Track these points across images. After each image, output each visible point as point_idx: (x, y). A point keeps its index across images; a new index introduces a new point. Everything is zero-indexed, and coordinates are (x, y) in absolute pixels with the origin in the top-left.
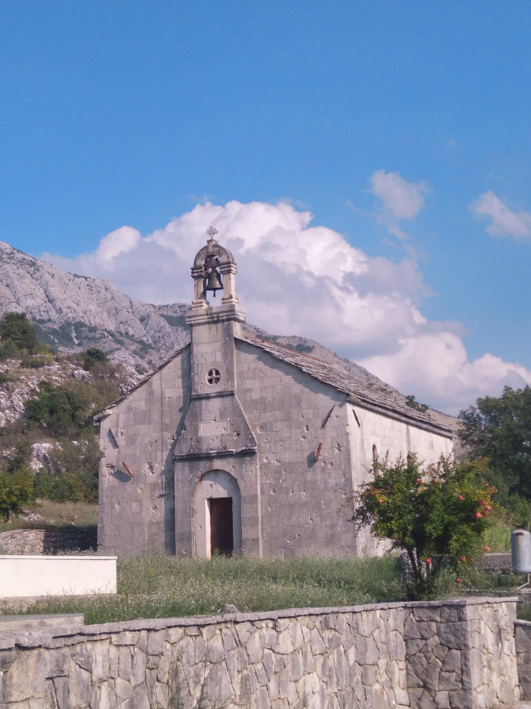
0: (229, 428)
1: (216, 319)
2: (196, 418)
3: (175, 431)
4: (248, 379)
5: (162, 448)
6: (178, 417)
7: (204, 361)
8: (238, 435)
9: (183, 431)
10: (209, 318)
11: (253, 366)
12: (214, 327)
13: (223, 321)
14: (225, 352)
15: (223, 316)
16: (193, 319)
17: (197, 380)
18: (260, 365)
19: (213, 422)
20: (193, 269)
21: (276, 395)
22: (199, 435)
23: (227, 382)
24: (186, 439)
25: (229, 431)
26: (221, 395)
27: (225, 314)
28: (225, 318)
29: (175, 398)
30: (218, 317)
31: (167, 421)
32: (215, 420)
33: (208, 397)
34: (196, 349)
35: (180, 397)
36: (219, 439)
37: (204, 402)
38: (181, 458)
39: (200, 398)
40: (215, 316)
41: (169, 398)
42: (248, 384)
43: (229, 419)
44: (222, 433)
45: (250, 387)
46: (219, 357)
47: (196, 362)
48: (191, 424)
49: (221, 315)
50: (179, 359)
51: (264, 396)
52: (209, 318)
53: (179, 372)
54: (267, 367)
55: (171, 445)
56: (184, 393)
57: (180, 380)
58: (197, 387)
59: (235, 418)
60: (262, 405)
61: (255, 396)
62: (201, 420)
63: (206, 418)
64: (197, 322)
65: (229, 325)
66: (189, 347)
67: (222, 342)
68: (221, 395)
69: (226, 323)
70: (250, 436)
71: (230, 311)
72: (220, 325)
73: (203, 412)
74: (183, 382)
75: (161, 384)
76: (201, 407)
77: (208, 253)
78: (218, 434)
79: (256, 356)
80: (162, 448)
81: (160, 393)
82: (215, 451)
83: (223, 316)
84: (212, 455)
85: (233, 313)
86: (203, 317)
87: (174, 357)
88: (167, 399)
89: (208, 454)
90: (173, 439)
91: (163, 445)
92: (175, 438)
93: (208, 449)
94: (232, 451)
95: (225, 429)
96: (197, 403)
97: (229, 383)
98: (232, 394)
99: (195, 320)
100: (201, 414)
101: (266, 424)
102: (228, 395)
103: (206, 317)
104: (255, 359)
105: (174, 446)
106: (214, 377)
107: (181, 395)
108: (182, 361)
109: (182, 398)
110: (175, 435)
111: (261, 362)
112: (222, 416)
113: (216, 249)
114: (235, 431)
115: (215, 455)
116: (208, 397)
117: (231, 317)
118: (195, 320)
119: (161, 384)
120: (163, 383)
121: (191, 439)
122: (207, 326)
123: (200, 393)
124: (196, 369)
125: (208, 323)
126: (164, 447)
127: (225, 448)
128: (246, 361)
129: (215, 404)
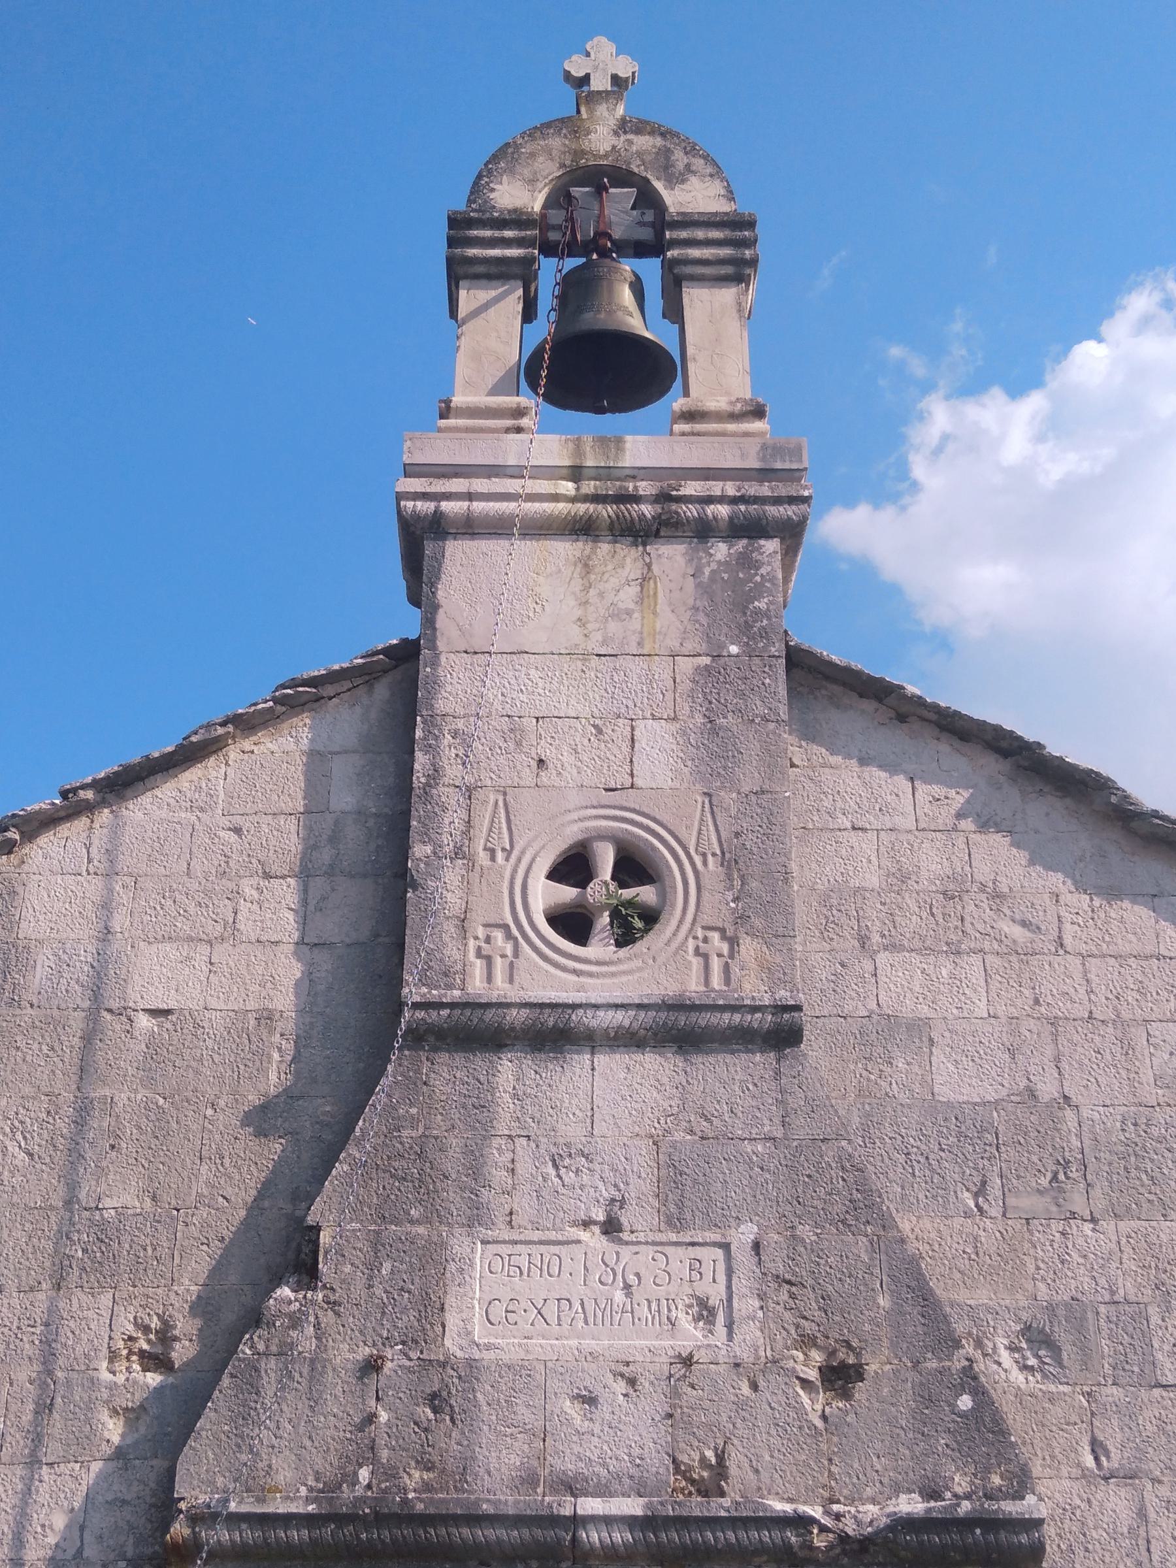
0: (747, 1304)
1: (647, 510)
2: (435, 1194)
3: (189, 1287)
4: (893, 947)
5: (37, 1439)
6: (227, 1179)
7: (528, 777)
8: (840, 1377)
9: (285, 1292)
10: (596, 499)
11: (932, 862)
12: (619, 565)
13: (704, 531)
14: (712, 728)
15: (709, 500)
16: (457, 485)
17: (454, 900)
18: (998, 858)
19: (593, 1239)
20: (456, 222)
21: (1151, 1093)
22: (452, 1344)
23: (733, 942)
24: (316, 1365)
25: (750, 1334)
26: (677, 1030)
27: (731, 489)
28: (723, 510)
29: (216, 1022)
30: (664, 498)
31: (120, 1195)
32: (611, 1228)
33: (553, 1034)
34: (453, 685)
35: (266, 1017)
36: (653, 1402)
37: (509, 1071)
38: (250, 1535)
39: (479, 1033)
40: (645, 488)
41: (155, 1013)
42: (900, 984)
43: (746, 1233)
44: (684, 1345)
45: (909, 1008)
46: (660, 759)
47: (453, 772)
48: (376, 1242)
49: (691, 488)
50: (287, 747)
51: (1047, 1089)
52: (596, 499)
53: (287, 840)
54: (1056, 880)
55: (133, 1416)
56: (308, 987)
57: (287, 892)
58: (452, 952)
59: (806, 1231)
60: (1021, 1148)
61: (958, 1080)
62: (477, 1217)
63: (524, 1205)
64: (478, 506)
65: (746, 562)
66: (406, 656)
67: (686, 665)
68: (677, 1030)
69: (721, 550)
70: (965, 1402)
71: (765, 474)
72: (671, 556)
73: (497, 1155)
74: (307, 911)
75: (106, 906)
76: (480, 1108)
77: (579, 153)
78: (648, 1344)
79: (959, 798)
80: (37, 1439)
81: (83, 971)
82: (633, 1506)
83: (709, 500)
84: (593, 1536)
85: (783, 490)
86: (543, 486)
87: (246, 724)
88: (144, 1022)
89: (554, 1521)
90: (156, 1361)
91: (44, 1407)
92: (182, 1352)
93: (530, 1480)
94: (802, 1522)
95: (705, 1312)
96: (447, 1074)
97: (749, 947)
98: (781, 1034)
99: (470, 497)
100: (476, 1170)
101: (1076, 1312)
102: (742, 1039)
103: (568, 487)
104: (945, 817)
105: (167, 1426)
106: (609, 888)
107: (285, 1001)
108: (316, 759)
109: (288, 1024)
110: (185, 1326)
111: (999, 841)
112: (683, 1199)
113: (643, 142)
114: (806, 1342)
115: (620, 1536)
116: (553, 1034)
117: (772, 511)
118: (470, 497)
119: (106, 906)
120: (123, 896)
121: (372, 1366)
122: (564, 549)
123: (477, 986)
124: (452, 821)
125: (582, 529)
126: (57, 1424)
127: (715, 1479)
128: (870, 820)
129: (615, 1100)
